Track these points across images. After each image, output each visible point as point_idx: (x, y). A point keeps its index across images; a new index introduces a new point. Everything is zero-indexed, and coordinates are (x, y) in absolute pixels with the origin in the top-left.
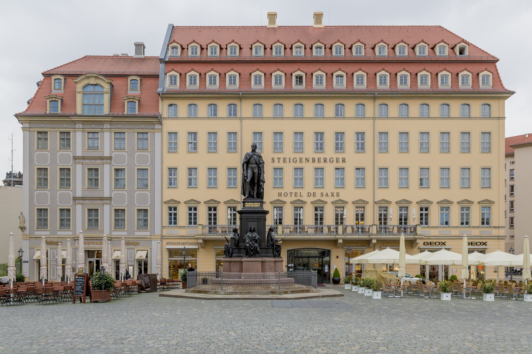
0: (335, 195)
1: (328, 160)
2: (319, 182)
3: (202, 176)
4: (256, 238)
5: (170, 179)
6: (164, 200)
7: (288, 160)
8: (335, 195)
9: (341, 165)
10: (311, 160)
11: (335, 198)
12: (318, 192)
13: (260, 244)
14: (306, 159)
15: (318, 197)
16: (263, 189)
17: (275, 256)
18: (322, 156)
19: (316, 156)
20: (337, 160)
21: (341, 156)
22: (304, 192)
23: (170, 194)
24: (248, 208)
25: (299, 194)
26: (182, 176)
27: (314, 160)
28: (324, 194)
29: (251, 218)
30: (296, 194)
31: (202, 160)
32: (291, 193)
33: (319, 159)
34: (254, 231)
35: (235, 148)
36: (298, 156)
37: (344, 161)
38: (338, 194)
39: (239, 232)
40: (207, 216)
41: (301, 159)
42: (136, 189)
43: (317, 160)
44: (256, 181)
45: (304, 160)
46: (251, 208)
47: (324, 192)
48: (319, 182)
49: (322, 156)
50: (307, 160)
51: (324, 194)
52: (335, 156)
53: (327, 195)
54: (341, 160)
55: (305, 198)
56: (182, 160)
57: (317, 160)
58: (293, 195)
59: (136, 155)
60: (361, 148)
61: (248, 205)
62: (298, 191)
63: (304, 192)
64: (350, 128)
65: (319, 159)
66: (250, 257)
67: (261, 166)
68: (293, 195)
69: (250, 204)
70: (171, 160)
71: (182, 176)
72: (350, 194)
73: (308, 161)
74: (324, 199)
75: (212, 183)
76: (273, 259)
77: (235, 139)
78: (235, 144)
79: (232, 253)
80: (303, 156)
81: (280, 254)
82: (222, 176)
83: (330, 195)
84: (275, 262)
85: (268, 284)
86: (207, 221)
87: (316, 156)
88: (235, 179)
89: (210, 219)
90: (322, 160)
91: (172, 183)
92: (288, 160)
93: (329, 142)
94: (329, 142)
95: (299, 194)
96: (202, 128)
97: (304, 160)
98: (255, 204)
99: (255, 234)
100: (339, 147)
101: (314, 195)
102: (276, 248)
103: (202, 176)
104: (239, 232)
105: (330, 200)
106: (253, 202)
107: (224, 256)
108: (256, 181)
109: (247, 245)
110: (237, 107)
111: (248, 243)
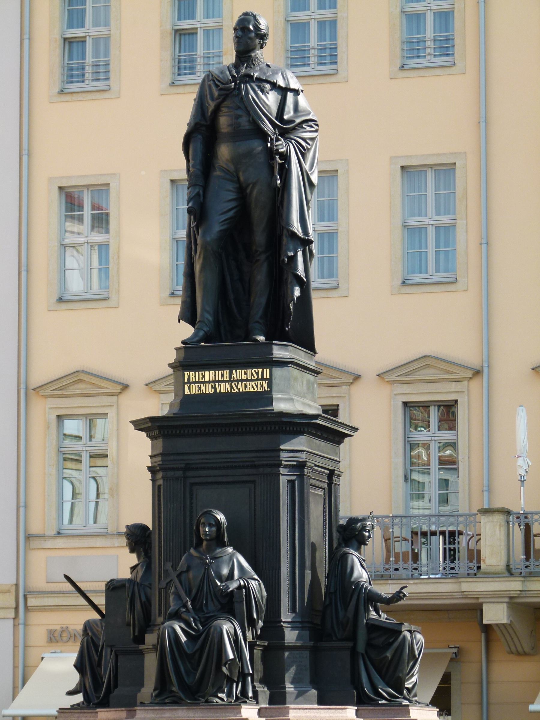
24: (202, 398)
29: (224, 460)
35: (445, 47)
44: (260, 237)
46: (217, 397)
69: (210, 375)
79: (114, 684)
88: (445, 232)
98: (238, 374)
106: (232, 366)
107: (79, 698)
108: (260, 237)
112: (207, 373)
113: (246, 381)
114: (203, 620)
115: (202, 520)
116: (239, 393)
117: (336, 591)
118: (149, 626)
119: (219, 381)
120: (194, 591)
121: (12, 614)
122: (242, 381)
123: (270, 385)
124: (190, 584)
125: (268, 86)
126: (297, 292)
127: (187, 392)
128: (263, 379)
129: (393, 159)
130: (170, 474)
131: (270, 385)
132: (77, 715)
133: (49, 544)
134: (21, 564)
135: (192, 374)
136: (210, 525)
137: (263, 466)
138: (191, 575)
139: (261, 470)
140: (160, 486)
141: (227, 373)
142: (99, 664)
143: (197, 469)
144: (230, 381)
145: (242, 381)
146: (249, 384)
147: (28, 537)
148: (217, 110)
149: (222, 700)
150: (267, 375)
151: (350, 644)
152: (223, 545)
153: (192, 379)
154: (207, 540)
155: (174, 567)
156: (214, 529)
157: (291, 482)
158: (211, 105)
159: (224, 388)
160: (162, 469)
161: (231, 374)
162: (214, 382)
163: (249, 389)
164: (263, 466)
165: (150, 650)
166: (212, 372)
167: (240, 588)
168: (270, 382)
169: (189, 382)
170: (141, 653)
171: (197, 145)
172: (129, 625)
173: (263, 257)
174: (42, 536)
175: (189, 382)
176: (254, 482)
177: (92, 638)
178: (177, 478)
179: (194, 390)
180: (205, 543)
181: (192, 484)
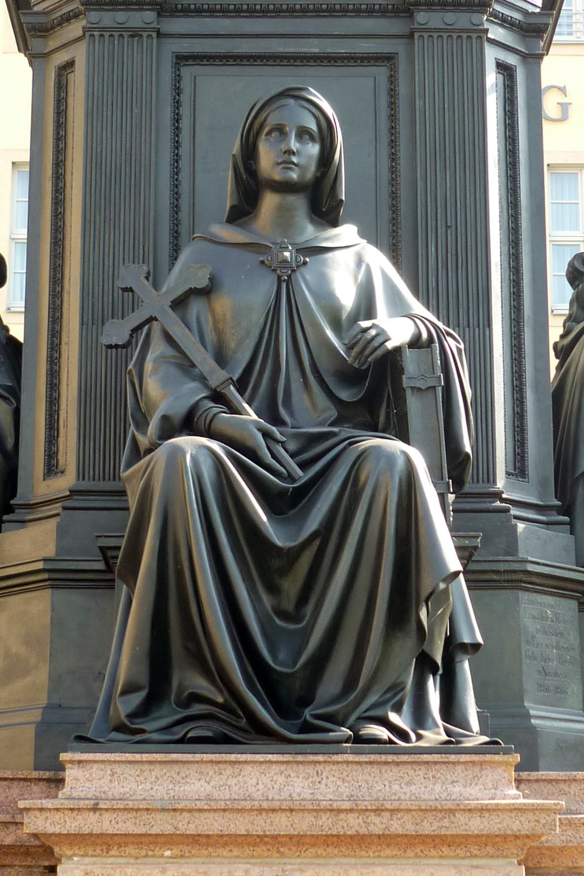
13: (456, 469)
66: (231, 729)
114: (292, 446)
115: (273, 120)
118: (10, 510)
120: (243, 358)
124: (219, 333)
136: (303, 133)
138: (223, 303)
149: (403, 735)
152: (326, 212)
154: (285, 187)
155: (155, 279)
156: (314, 149)
176: (388, 59)
178: (135, 34)
180: (270, 201)
181: (181, 59)
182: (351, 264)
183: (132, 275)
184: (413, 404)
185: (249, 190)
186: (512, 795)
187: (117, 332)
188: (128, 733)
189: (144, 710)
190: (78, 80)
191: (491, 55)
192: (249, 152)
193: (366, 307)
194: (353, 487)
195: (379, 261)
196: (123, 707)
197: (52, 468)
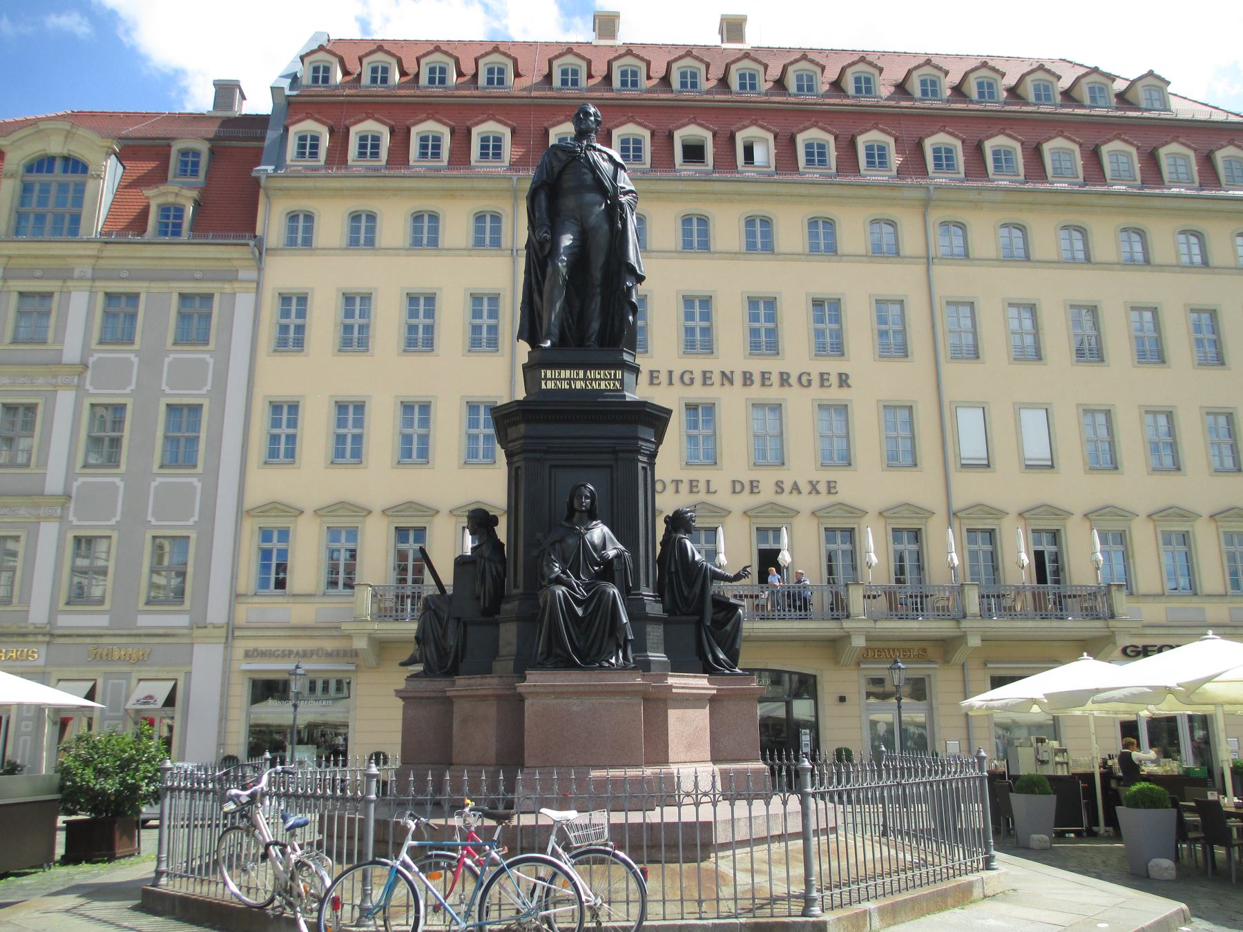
0: (822, 487)
1: (793, 380)
2: (769, 450)
3: (382, 430)
4: (611, 553)
5: (275, 439)
6: (249, 502)
7: (664, 377)
8: (822, 487)
9: (834, 394)
10: (738, 379)
11: (823, 500)
12: (767, 479)
14: (723, 373)
15: (767, 493)
16: (634, 309)
17: (708, 669)
18: (773, 366)
19: (757, 366)
20: (823, 378)
21: (832, 366)
22: (720, 479)
23: (269, 483)
25: (702, 486)
26: (316, 430)
27: (747, 379)
28: (787, 486)
30: (693, 485)
31: (384, 376)
32: (677, 482)
33: (765, 376)
34: (592, 515)
36: (697, 365)
37: (843, 380)
38: (831, 487)
39: (501, 532)
40: (392, 560)
41: (706, 377)
42: (155, 469)
43: (757, 378)
44: (597, 274)
45: (716, 377)
47: (787, 477)
48: (769, 450)
49: (773, 366)
50: (727, 378)
51: (787, 486)
52: (816, 367)
53: (796, 488)
54: (834, 380)
55: (723, 497)
56: (316, 377)
57: (757, 378)
58: (684, 488)
59: (167, 360)
60: (893, 345)
61: (553, 379)
62: (701, 475)
63: (720, 479)
64: (857, 284)
65: (765, 376)
66: (569, 665)
67: (623, 199)
68: (684, 488)
69: (566, 373)
70: (281, 376)
71: (316, 430)
72: (870, 486)
73: (731, 383)
74: (786, 500)
75: (414, 449)
76: (699, 683)
77: (494, 314)
78: (493, 329)
80: (715, 365)
81: (734, 657)
82: (449, 429)
83: (805, 488)
84: (712, 700)
85: (694, 843)
86: (392, 577)
87: (757, 366)
89: (402, 569)
90: (775, 379)
91: (283, 449)
92: (664, 377)
93: (796, 327)
94: (796, 327)
95: (702, 486)
96: (389, 276)
97: (716, 377)
99: (598, 532)
100: (831, 343)
101: (754, 487)
102: (713, 621)
103: (382, 430)
104: (501, 532)
105: (805, 502)
106: (586, 366)
107: (419, 668)
108: (597, 274)
109: (560, 590)
110: (504, 220)
111: (558, 581)
112: (563, 372)
113: (600, 380)
116: (593, 389)
117: (677, 571)
119: (574, 379)
121: (224, 640)
122: (596, 380)
123: (622, 384)
125: (605, 156)
126: (631, 318)
127: (543, 386)
128: (615, 379)
129: (462, 397)
130: (531, 455)
131: (622, 384)
132: (424, 683)
133: (250, 600)
134: (231, 612)
135: (549, 372)
136: (587, 497)
137: (622, 451)
139: (620, 455)
140: (517, 469)
141: (581, 373)
142: (445, 636)
143: (557, 452)
144: (585, 379)
145: (596, 380)
146: (603, 383)
147: (238, 596)
148: (561, 172)
150: (619, 375)
151: (697, 618)
153: (549, 376)
157: (645, 469)
158: (557, 166)
159: (579, 385)
160: (524, 451)
161: (585, 374)
162: (570, 379)
163: (603, 387)
164: (622, 451)
165: (508, 620)
166: (568, 372)
167: (618, 556)
168: (622, 381)
169: (546, 379)
170: (496, 624)
171: (542, 198)
172: (479, 598)
173: (598, 290)
174: (245, 595)
175: (546, 379)
176: (611, 467)
177: (434, 611)
179: (551, 385)
180: (577, 514)
181: (552, 467)
182: (598, 532)
183: (539, 535)
184: (616, 574)
185: (572, 511)
186: (639, 680)
187: (535, 552)
188: (540, 666)
189: (546, 659)
190: (522, 472)
191: (640, 465)
192: (571, 501)
193: (604, 547)
194: (600, 601)
195: (606, 529)
196: (539, 659)
197: (516, 586)
